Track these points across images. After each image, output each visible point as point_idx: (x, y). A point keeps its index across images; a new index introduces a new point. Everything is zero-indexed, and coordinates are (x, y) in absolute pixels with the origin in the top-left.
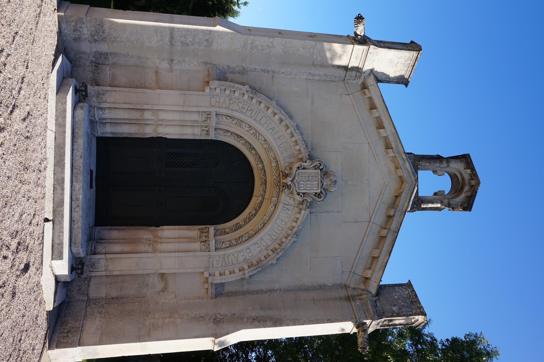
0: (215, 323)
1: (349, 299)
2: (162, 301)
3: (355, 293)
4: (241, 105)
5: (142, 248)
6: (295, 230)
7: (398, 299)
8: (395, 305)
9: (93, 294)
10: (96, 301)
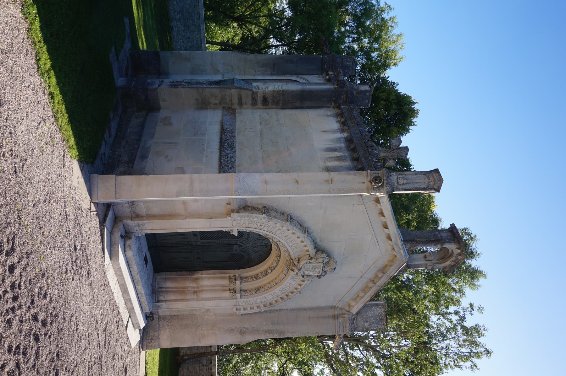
0: (240, 334)
1: (335, 317)
2: (207, 317)
3: (341, 312)
4: (259, 224)
5: (189, 297)
6: (298, 290)
7: (372, 317)
8: (367, 322)
9: (161, 314)
10: (164, 317)
